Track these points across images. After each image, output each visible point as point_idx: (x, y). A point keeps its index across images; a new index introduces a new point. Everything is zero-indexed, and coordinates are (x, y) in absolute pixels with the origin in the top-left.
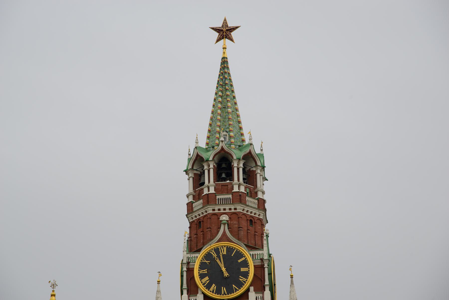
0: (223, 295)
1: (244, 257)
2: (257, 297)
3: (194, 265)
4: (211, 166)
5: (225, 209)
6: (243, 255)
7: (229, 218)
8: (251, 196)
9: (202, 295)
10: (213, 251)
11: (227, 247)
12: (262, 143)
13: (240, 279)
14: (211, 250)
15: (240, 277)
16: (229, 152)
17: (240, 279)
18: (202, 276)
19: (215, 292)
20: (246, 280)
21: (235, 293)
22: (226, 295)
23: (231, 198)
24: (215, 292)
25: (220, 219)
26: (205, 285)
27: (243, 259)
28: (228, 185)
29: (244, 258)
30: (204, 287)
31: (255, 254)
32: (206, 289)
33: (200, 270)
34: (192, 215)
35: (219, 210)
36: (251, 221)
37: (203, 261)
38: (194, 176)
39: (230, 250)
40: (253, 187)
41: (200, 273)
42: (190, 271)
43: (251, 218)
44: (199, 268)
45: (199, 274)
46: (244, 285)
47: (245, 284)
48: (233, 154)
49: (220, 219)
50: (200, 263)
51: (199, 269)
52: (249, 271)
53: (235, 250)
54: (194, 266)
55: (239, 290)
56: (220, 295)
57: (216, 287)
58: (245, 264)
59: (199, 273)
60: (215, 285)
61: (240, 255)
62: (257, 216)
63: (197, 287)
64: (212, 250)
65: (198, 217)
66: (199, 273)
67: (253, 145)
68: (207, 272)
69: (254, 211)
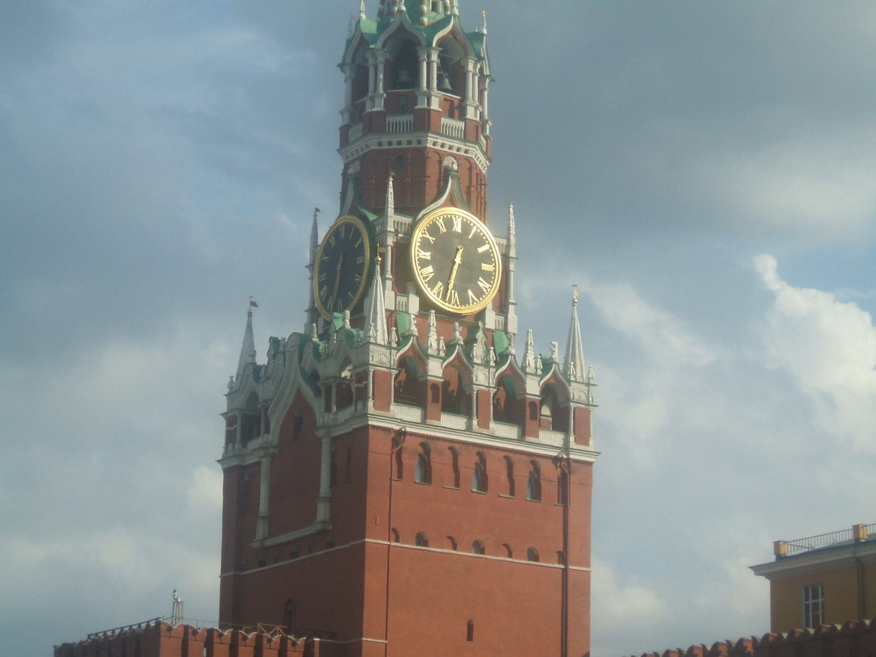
5: (451, 148)
60: (441, 284)
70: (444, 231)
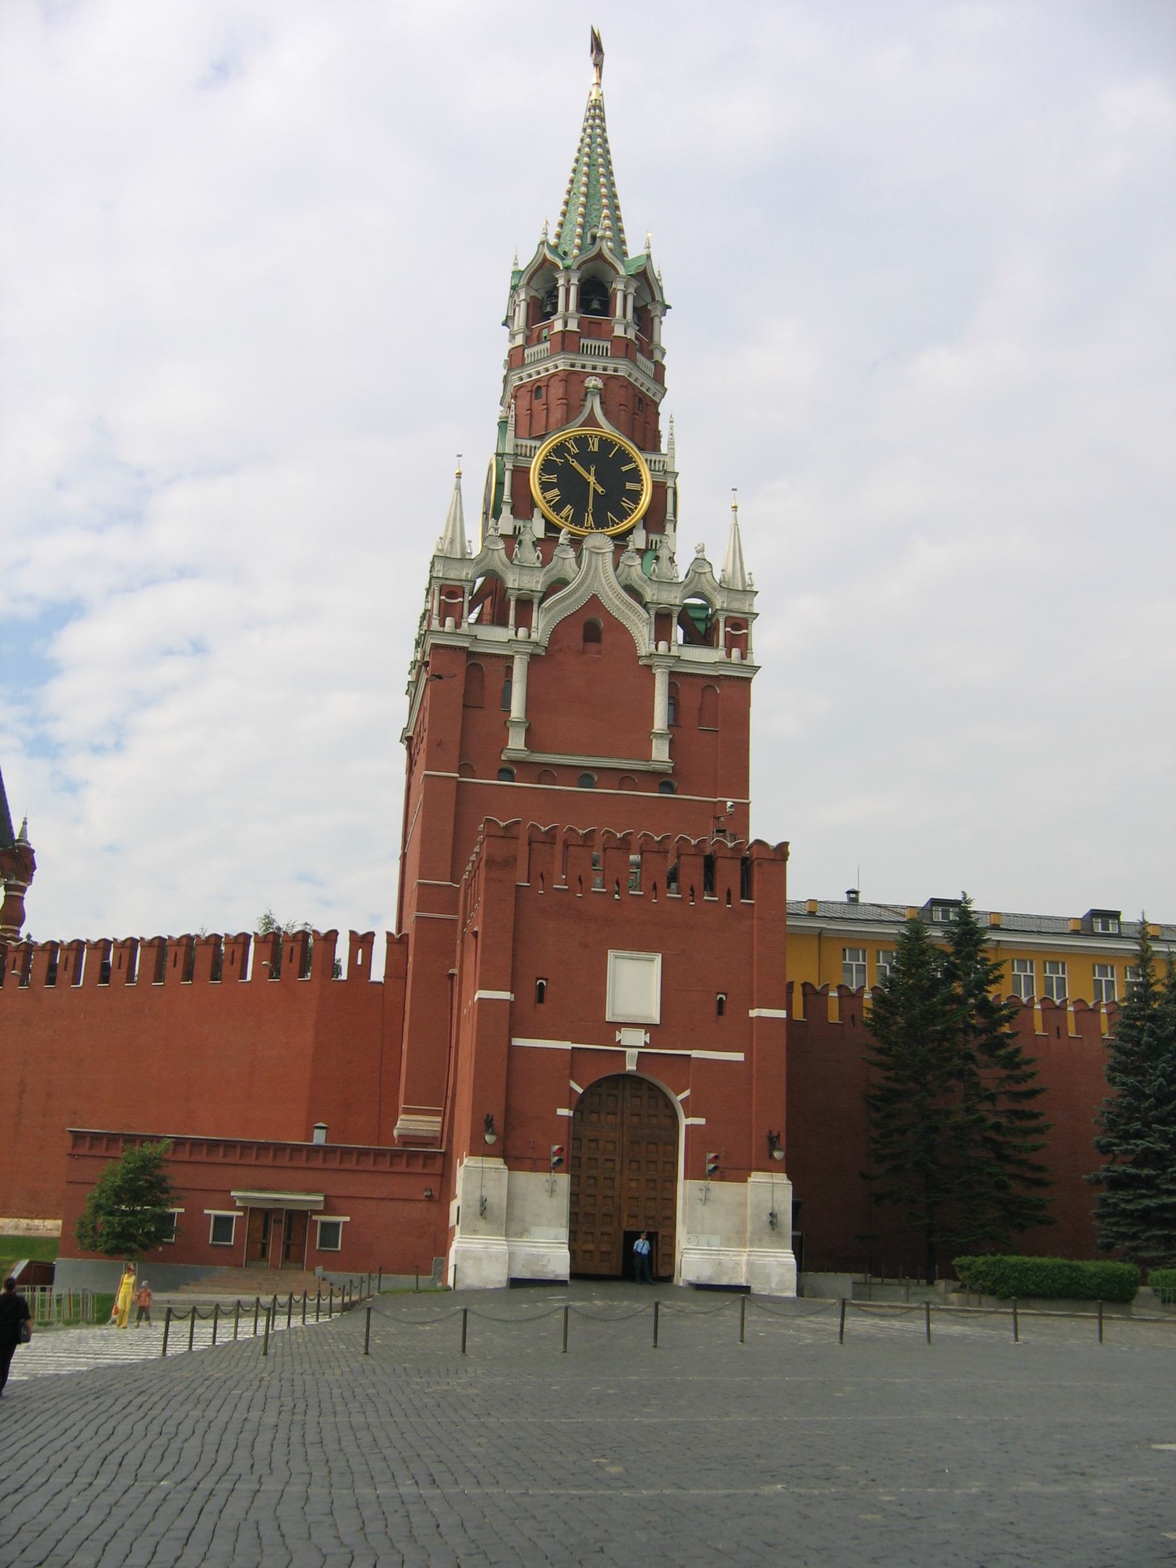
4: (574, 281)
5: (594, 368)
6: (632, 458)
9: (543, 521)
13: (623, 504)
15: (624, 499)
17: (623, 504)
18: (545, 487)
20: (636, 508)
23: (609, 347)
25: (586, 385)
27: (632, 466)
30: (550, 507)
31: (659, 461)
34: (522, 373)
35: (583, 367)
36: (640, 399)
42: (521, 474)
44: (541, 469)
46: (630, 515)
50: (544, 460)
52: (642, 490)
56: (581, 527)
58: (635, 476)
61: (627, 458)
63: (533, 505)
66: (540, 479)
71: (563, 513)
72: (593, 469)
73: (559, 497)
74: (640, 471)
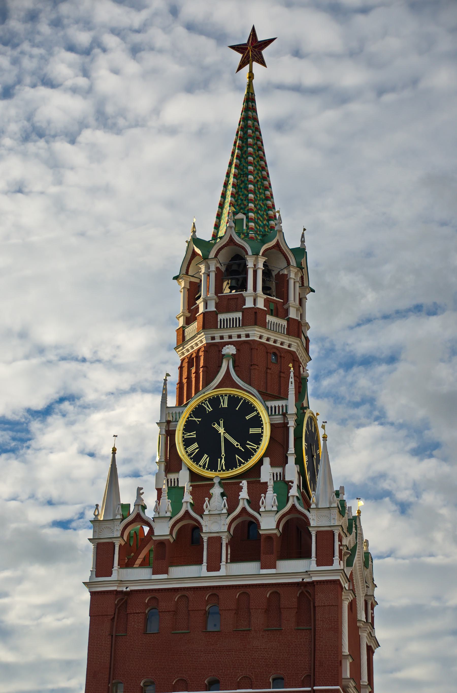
0: (220, 471)
1: (256, 410)
2: (273, 474)
3: (177, 425)
4: (213, 268)
6: (254, 407)
7: (237, 350)
8: (271, 314)
9: (188, 472)
10: (207, 402)
11: (230, 396)
12: (305, 230)
14: (204, 402)
16: (241, 244)
18: (187, 443)
19: (206, 467)
21: (239, 468)
22: (224, 471)
24: (206, 467)
25: (223, 353)
26: (192, 456)
27: (254, 414)
28: (238, 298)
29: (255, 412)
30: (191, 459)
32: (194, 462)
33: (185, 433)
34: (184, 348)
35: (222, 338)
37: (190, 419)
38: (190, 287)
39: (233, 400)
40: (282, 301)
41: (185, 437)
43: (275, 351)
44: (184, 429)
45: (183, 439)
47: (254, 453)
48: (247, 248)
49: (223, 353)
51: (184, 431)
53: (241, 401)
54: (176, 427)
55: (245, 462)
57: (208, 458)
58: (257, 422)
59: (183, 438)
60: (207, 456)
61: (249, 408)
62: (285, 347)
64: (206, 400)
65: (191, 351)
66: (183, 437)
67: (283, 233)
68: (195, 436)
69: (273, 336)
70: (210, 410)
71: (201, 463)
72: (222, 422)
73: (197, 450)
74: (260, 417)
